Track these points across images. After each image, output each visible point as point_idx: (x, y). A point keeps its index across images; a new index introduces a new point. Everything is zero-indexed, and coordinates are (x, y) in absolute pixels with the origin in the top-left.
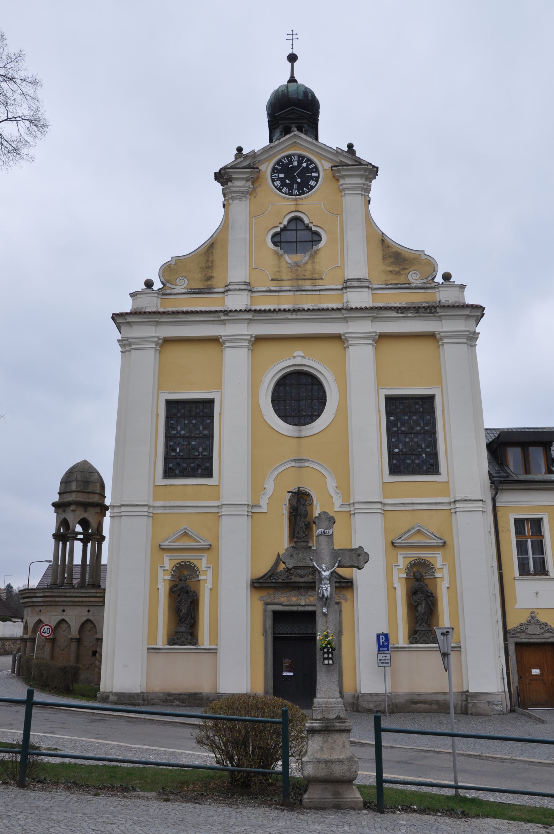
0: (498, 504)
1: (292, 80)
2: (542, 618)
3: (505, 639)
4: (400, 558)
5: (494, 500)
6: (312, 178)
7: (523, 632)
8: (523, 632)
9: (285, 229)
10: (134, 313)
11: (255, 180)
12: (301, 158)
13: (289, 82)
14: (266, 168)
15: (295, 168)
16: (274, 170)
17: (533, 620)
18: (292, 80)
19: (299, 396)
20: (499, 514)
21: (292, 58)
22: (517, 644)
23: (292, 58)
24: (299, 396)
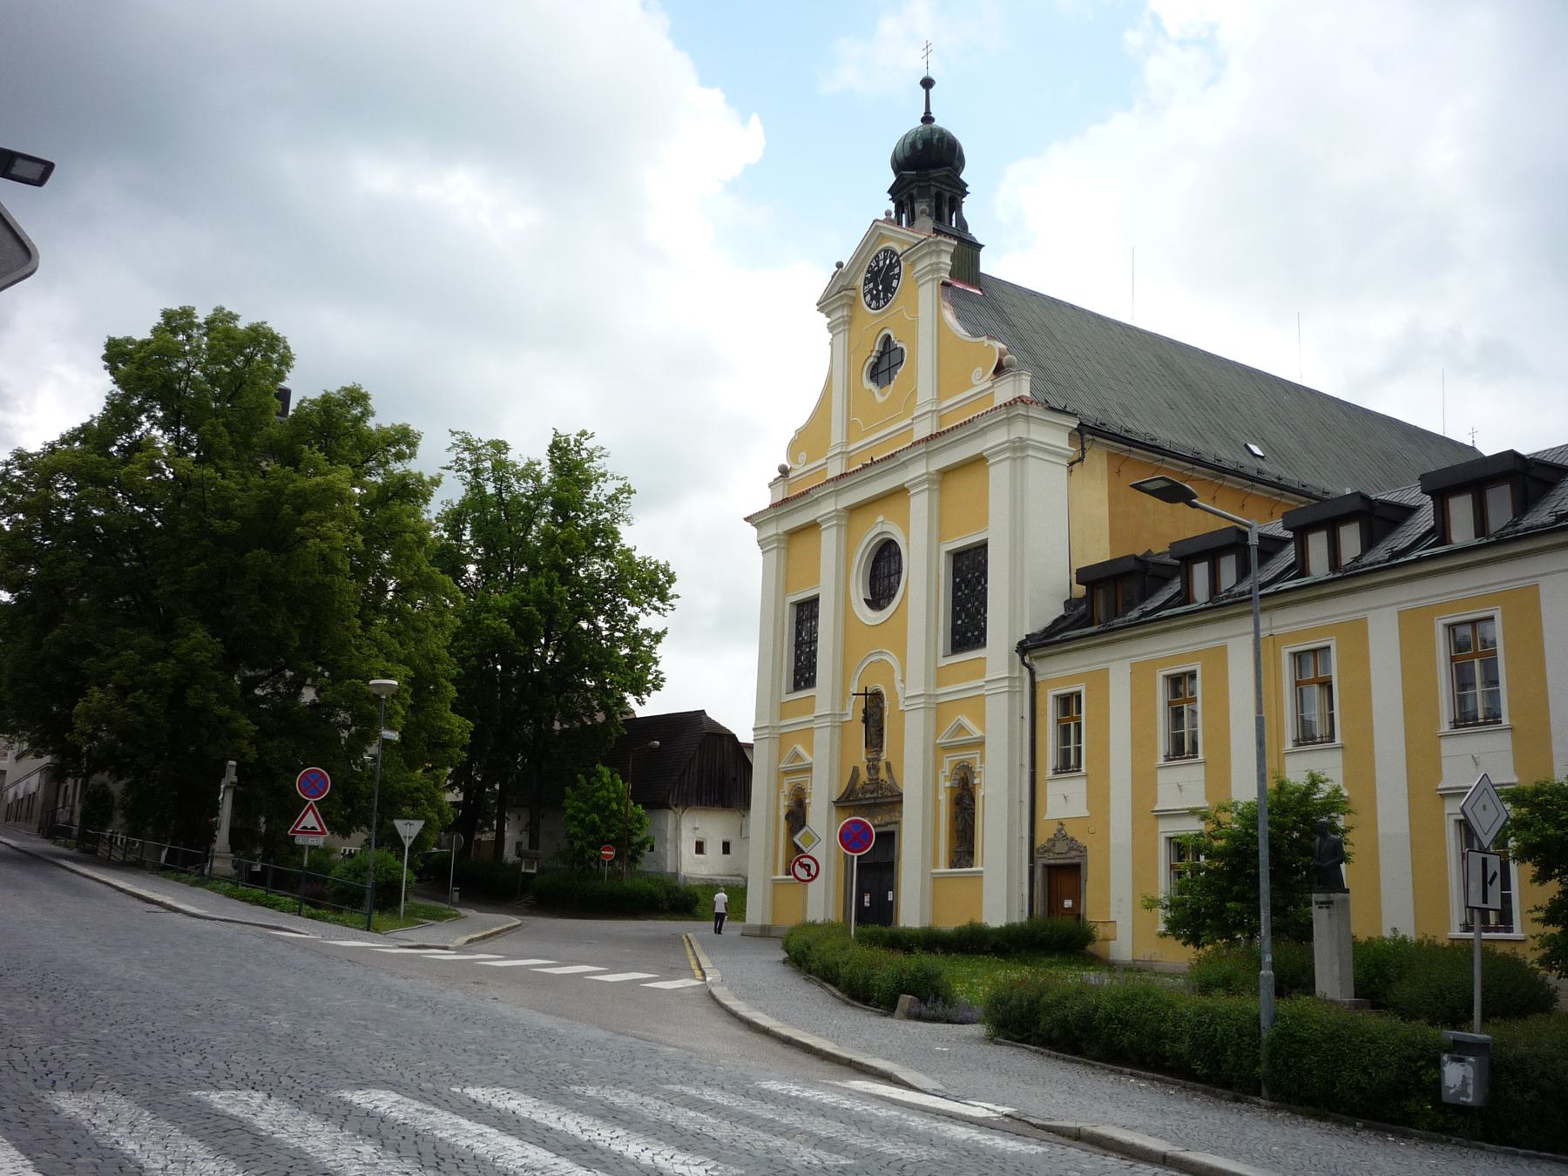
0: (1038, 679)
1: (927, 119)
2: (1070, 831)
3: (1032, 859)
4: (946, 762)
5: (1032, 674)
6: (893, 277)
7: (1048, 851)
8: (1048, 851)
9: (882, 354)
10: (773, 506)
11: (852, 304)
12: (886, 251)
13: (923, 120)
14: (860, 282)
15: (880, 270)
16: (867, 281)
17: (1060, 835)
18: (927, 119)
19: (884, 572)
20: (1039, 691)
21: (927, 83)
22: (1049, 868)
23: (927, 83)
24: (884, 572)
